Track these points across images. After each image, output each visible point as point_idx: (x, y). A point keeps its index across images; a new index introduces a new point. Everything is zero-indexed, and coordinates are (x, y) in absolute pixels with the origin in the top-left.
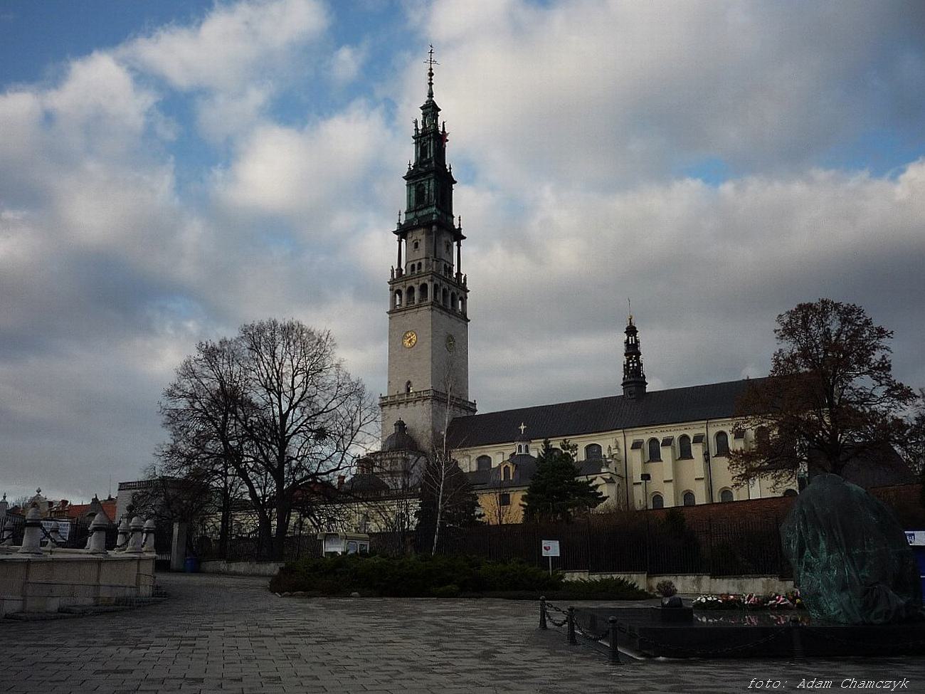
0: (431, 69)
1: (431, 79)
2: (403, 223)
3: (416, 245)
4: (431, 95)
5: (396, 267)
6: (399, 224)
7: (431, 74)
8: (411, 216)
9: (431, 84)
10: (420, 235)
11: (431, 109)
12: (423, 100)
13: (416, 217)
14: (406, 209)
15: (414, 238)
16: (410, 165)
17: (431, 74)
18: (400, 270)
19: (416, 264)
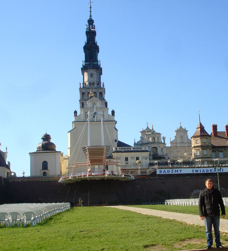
0: (90, 6)
1: (91, 10)
2: (84, 65)
3: (92, 75)
4: (91, 16)
5: (82, 82)
6: (83, 65)
7: (91, 8)
8: (88, 63)
9: (91, 11)
10: (93, 71)
11: (91, 22)
12: (88, 18)
13: (90, 64)
14: (84, 60)
15: (91, 72)
16: (85, 42)
17: (91, 8)
18: (84, 83)
19: (92, 82)
